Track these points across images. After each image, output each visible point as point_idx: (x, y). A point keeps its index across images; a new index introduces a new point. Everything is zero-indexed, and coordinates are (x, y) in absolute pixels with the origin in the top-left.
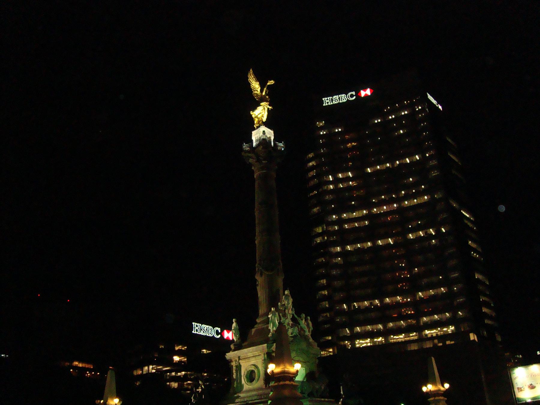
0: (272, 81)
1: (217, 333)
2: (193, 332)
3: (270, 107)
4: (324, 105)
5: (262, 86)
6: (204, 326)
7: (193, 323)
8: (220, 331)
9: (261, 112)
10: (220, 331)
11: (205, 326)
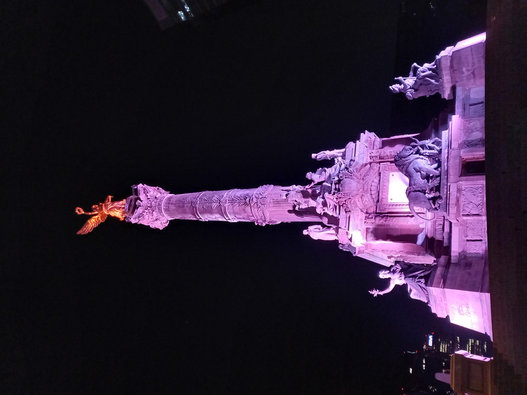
0: (77, 211)
5: (90, 217)
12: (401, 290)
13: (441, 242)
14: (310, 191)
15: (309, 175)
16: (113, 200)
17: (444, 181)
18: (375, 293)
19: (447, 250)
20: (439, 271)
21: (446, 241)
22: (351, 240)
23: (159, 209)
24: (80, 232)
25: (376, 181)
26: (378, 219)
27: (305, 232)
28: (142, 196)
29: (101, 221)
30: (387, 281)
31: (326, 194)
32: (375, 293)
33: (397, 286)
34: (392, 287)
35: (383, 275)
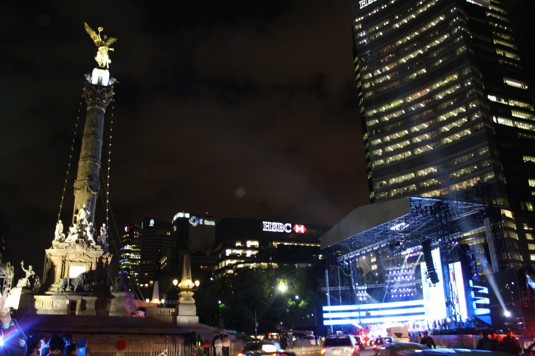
0: (100, 28)
1: (288, 228)
2: (264, 230)
4: (361, 8)
6: (274, 223)
7: (264, 222)
8: (291, 227)
9: (103, 57)
10: (291, 227)
11: (275, 224)
14: (84, 223)
16: (109, 53)
18: (22, 263)
21: (47, 293)
22: (53, 248)
25: (83, 260)
29: (95, 41)
30: (27, 268)
32: (22, 263)
33: (25, 273)
34: (26, 271)
35: (30, 267)
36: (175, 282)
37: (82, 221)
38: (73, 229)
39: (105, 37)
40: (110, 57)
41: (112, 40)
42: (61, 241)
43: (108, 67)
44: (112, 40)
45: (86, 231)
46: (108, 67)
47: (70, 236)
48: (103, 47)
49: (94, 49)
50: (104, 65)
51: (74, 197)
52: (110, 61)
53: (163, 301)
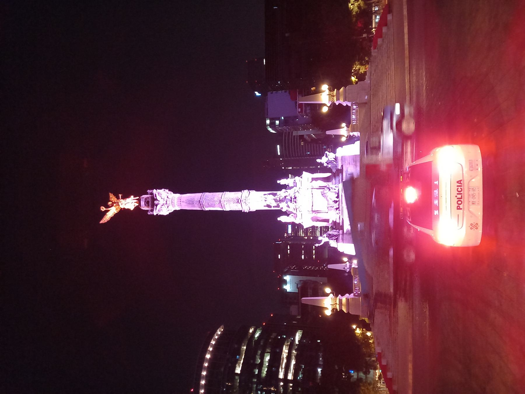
0: (102, 209)
3: (120, 195)
5: (109, 211)
9: (130, 203)
12: (327, 243)
13: (339, 223)
14: (278, 199)
15: (278, 193)
16: (124, 198)
17: (340, 204)
19: (342, 228)
20: (341, 236)
21: (341, 224)
23: (173, 205)
24: (101, 222)
26: (314, 214)
27: (279, 219)
28: (158, 198)
30: (321, 241)
31: (289, 203)
36: (325, 110)
37: (276, 200)
38: (283, 206)
39: (110, 203)
40: (128, 197)
41: (113, 198)
42: (296, 217)
43: (138, 198)
44: (113, 198)
45: (285, 197)
46: (138, 198)
47: (290, 210)
48: (120, 204)
49: (123, 212)
50: (136, 201)
51: (258, 211)
52: (132, 197)
53: (344, 125)
